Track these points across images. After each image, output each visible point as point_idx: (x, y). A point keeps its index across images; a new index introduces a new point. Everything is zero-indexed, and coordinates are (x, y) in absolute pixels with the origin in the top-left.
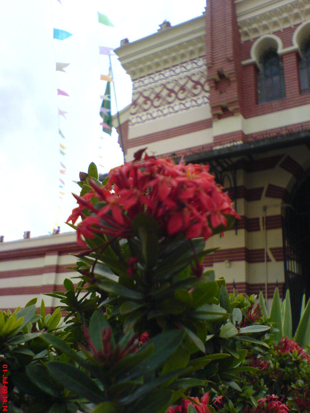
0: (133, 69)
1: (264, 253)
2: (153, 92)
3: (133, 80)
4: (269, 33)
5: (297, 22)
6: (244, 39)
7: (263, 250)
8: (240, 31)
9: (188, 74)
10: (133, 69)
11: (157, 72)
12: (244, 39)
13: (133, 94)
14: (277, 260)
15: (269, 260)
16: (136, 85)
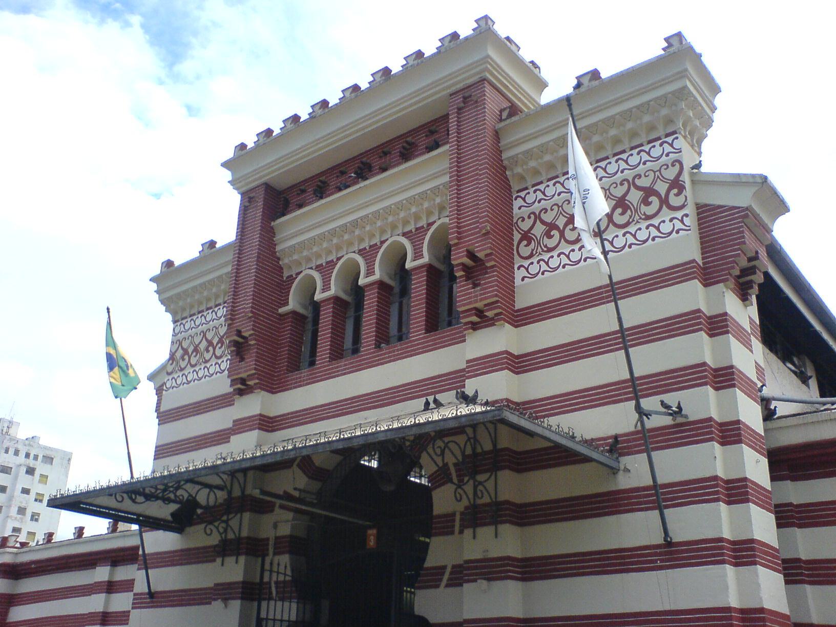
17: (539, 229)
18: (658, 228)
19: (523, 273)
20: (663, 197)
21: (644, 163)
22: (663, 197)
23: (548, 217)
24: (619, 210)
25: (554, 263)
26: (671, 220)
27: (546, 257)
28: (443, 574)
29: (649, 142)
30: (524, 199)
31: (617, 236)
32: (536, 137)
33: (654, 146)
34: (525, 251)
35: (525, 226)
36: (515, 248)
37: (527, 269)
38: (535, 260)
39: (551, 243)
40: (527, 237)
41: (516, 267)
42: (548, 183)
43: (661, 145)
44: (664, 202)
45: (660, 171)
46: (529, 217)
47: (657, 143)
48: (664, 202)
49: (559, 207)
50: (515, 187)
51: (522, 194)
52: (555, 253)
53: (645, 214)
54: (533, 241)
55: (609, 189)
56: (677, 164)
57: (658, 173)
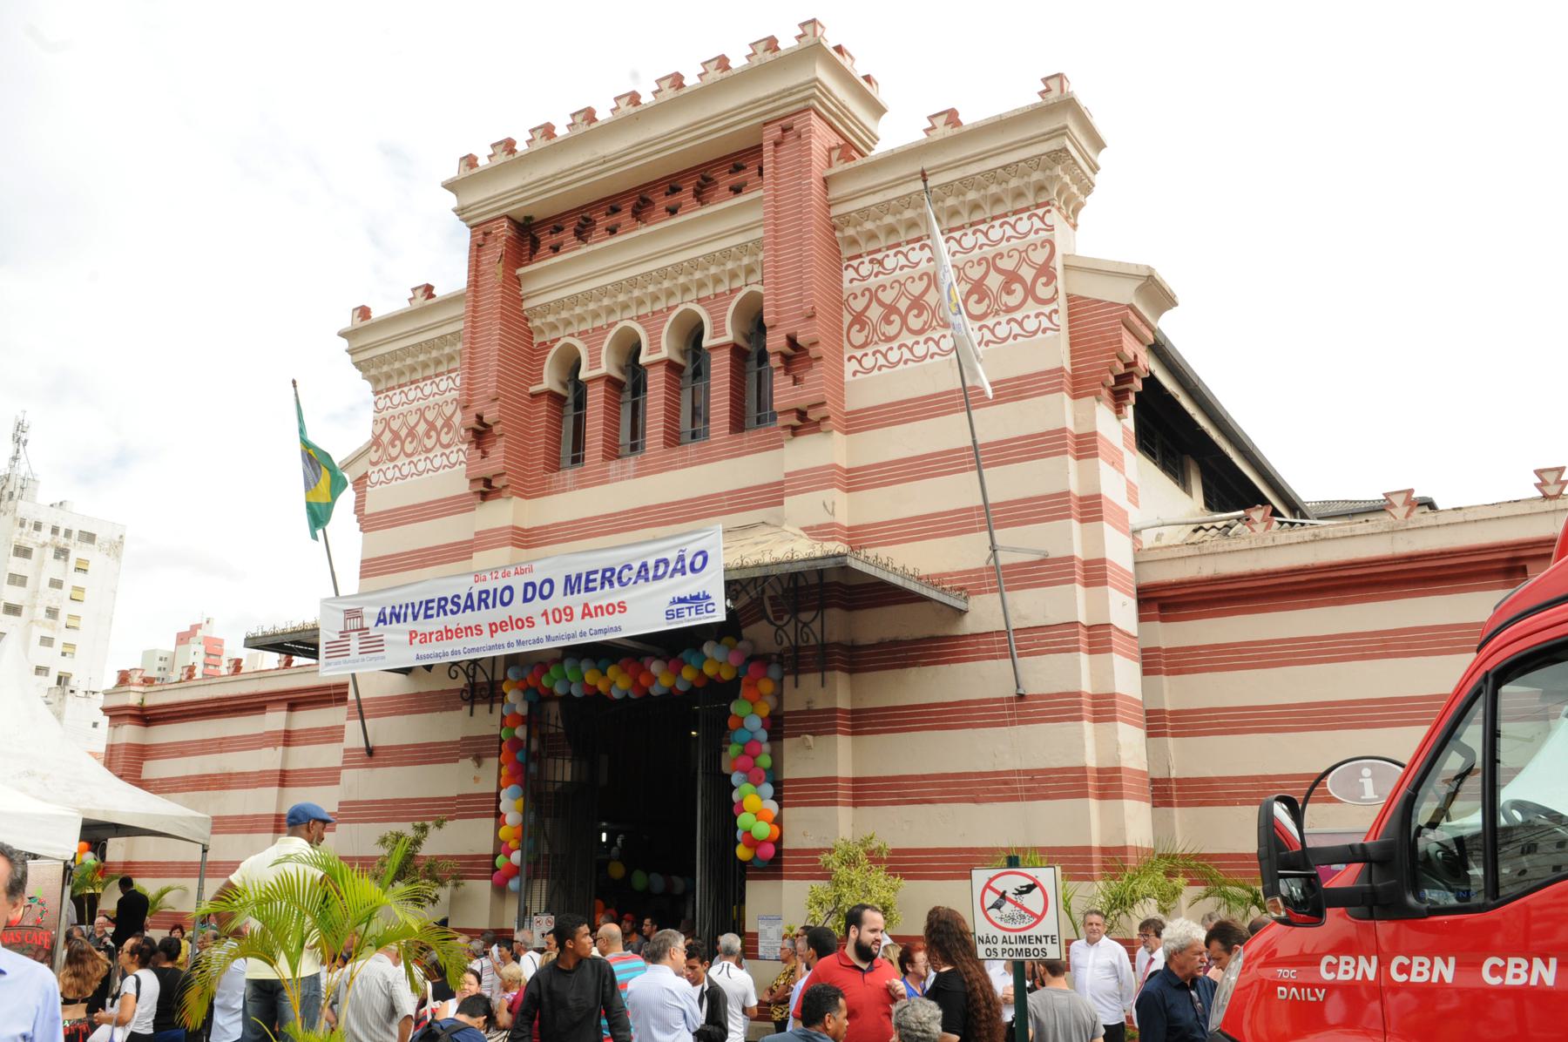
0: (373, 372)
2: (439, 414)
3: (376, 393)
4: (572, 335)
5: (611, 320)
6: (537, 340)
8: (530, 325)
10: (373, 372)
12: (537, 340)
13: (375, 421)
16: (381, 404)
17: (875, 312)
18: (1020, 324)
19: (854, 365)
20: (1029, 285)
21: (1008, 239)
22: (1029, 285)
23: (887, 297)
24: (975, 297)
25: (894, 356)
26: (1037, 316)
27: (883, 347)
29: (1015, 213)
30: (856, 270)
32: (874, 193)
33: (1021, 219)
34: (858, 338)
35: (858, 305)
36: (845, 333)
37: (860, 362)
38: (869, 350)
39: (891, 330)
40: (859, 319)
41: (846, 357)
42: (888, 252)
43: (1030, 218)
44: (1030, 292)
45: (1026, 251)
46: (863, 295)
47: (1025, 215)
48: (1030, 292)
50: (846, 253)
51: (855, 263)
52: (895, 344)
53: (1006, 305)
55: (963, 269)
56: (1048, 246)
57: (1024, 254)
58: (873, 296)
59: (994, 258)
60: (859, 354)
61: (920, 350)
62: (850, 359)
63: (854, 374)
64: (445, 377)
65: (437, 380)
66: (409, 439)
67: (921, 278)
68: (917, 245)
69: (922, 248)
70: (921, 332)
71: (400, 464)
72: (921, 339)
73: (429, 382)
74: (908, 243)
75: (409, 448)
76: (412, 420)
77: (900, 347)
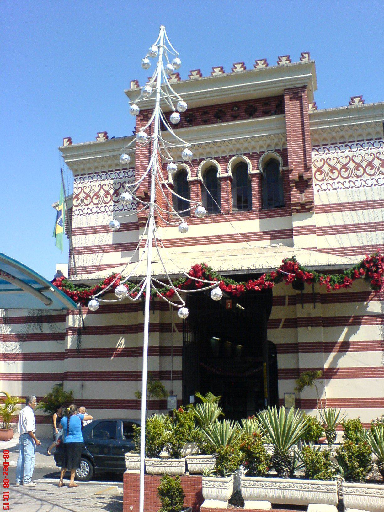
1: (171, 326)
7: (171, 324)
9: (122, 181)
11: (96, 173)
14: (179, 331)
15: (174, 331)
19: (318, 187)
23: (332, 163)
28: (280, 322)
31: (368, 179)
34: (320, 178)
35: (319, 164)
38: (325, 182)
40: (320, 170)
49: (337, 159)
52: (336, 181)
54: (323, 173)
55: (364, 156)
58: (325, 162)
59: (377, 154)
60: (320, 183)
61: (347, 185)
62: (316, 185)
63: (318, 191)
64: (113, 172)
65: (109, 173)
66: (95, 197)
67: (346, 157)
68: (344, 145)
69: (346, 146)
70: (347, 178)
71: (91, 208)
72: (347, 180)
73: (105, 174)
74: (340, 143)
75: (95, 201)
76: (97, 189)
77: (338, 183)
